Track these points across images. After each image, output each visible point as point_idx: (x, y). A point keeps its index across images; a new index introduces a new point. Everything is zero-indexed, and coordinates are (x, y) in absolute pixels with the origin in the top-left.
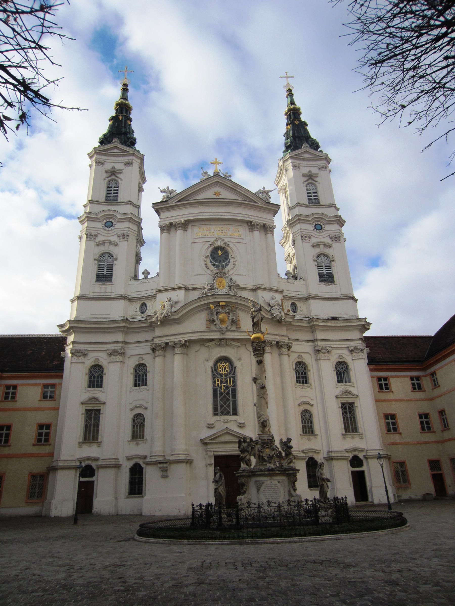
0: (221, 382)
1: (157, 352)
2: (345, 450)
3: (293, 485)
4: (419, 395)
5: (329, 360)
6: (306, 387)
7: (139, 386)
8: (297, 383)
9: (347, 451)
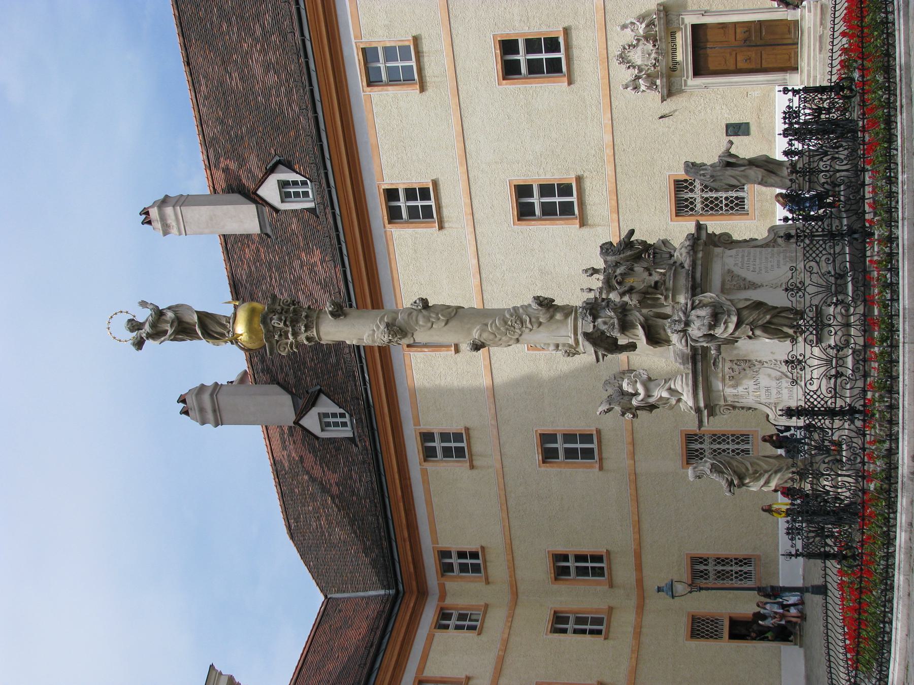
4: (495, 621)
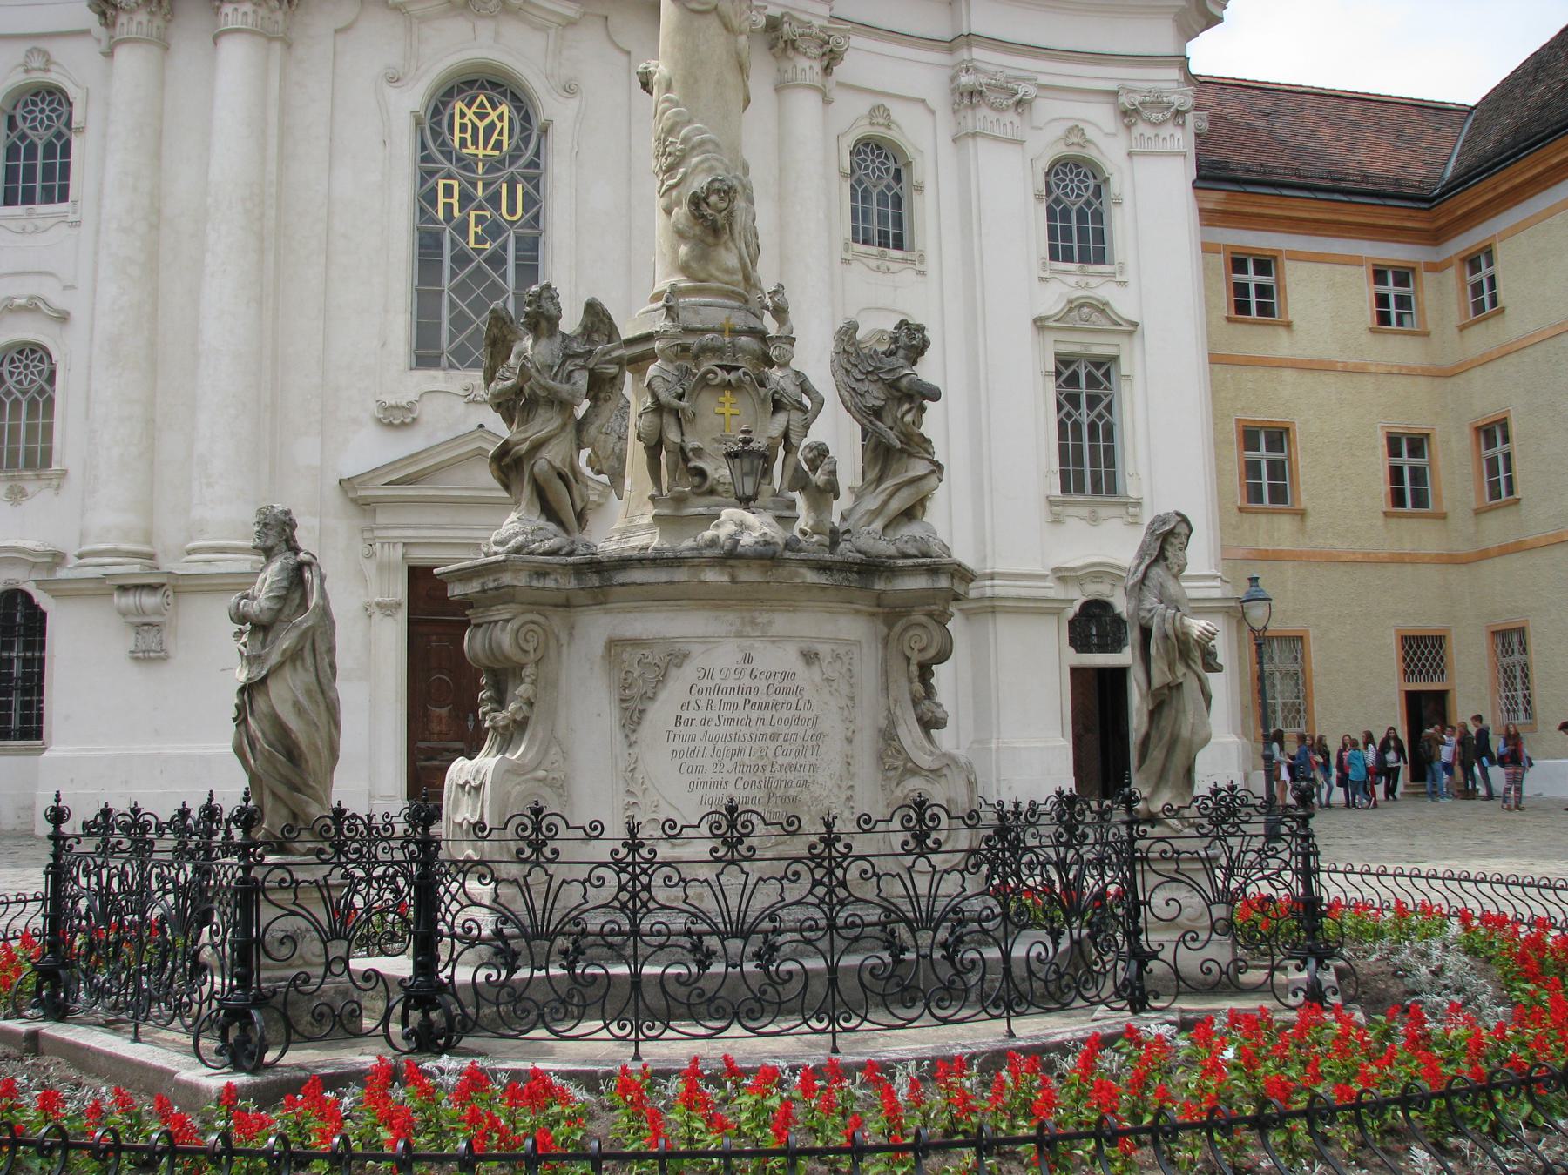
0: (466, 199)
1: (123, 19)
2: (1056, 570)
3: (918, 686)
4: (1397, 349)
5: (1021, 143)
6: (894, 267)
7: (29, 199)
8: (855, 240)
9: (1063, 576)
